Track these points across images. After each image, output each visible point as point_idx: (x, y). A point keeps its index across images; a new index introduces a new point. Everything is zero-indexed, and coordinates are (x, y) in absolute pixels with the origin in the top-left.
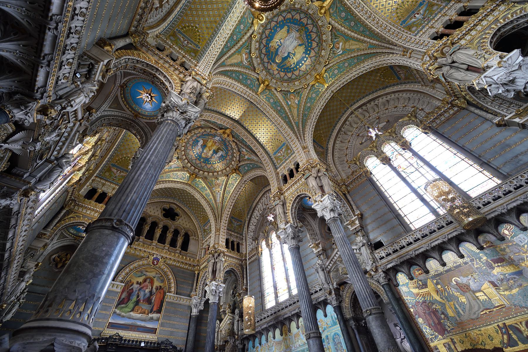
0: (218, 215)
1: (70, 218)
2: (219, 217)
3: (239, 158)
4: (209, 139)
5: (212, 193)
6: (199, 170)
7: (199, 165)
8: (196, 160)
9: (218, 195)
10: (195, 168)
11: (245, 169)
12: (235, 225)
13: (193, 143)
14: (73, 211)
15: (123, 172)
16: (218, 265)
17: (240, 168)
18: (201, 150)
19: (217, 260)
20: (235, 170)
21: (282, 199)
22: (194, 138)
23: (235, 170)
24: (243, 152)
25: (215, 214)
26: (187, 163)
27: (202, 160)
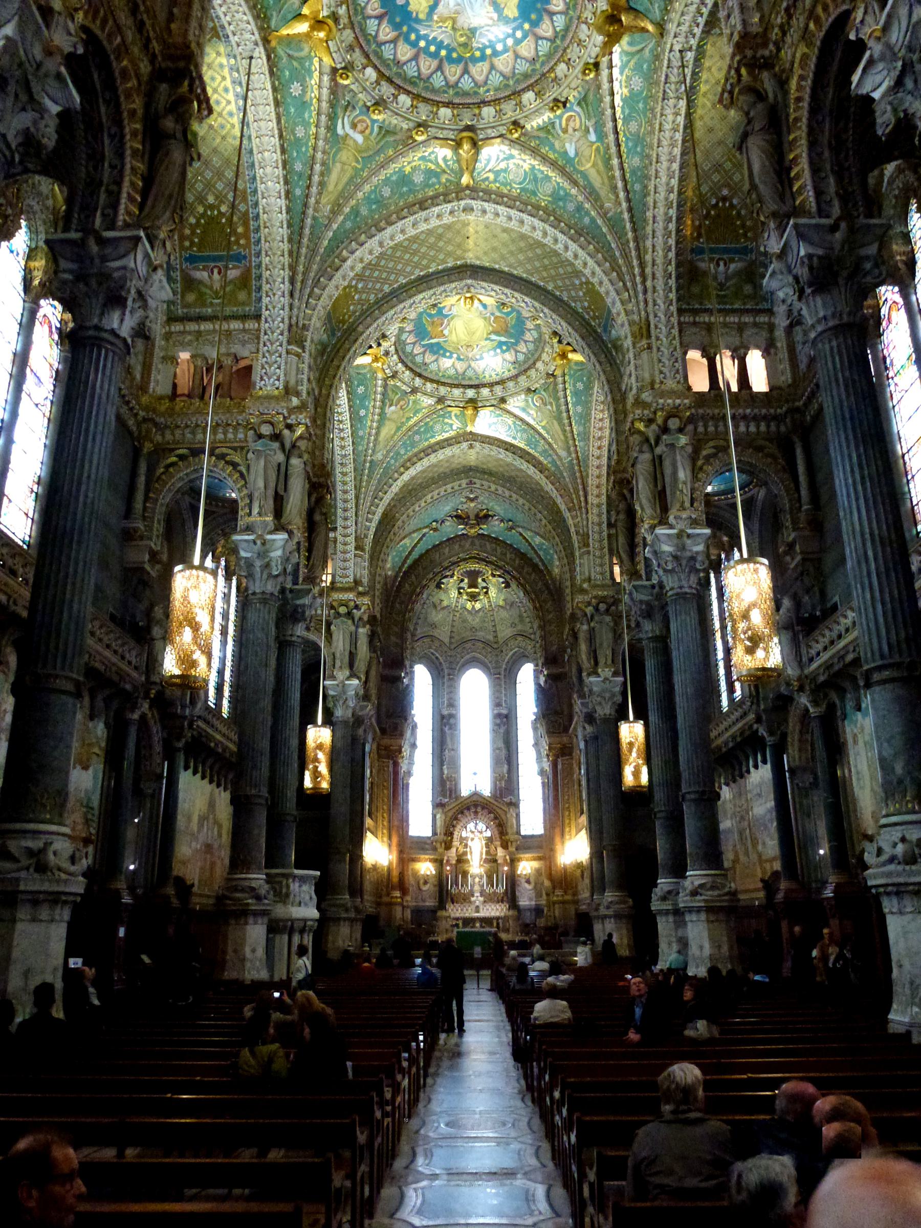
1: (167, 467)
8: (440, 68)
12: (721, 278)
14: (164, 450)
16: (667, 463)
19: (658, 450)
21: (771, 95)
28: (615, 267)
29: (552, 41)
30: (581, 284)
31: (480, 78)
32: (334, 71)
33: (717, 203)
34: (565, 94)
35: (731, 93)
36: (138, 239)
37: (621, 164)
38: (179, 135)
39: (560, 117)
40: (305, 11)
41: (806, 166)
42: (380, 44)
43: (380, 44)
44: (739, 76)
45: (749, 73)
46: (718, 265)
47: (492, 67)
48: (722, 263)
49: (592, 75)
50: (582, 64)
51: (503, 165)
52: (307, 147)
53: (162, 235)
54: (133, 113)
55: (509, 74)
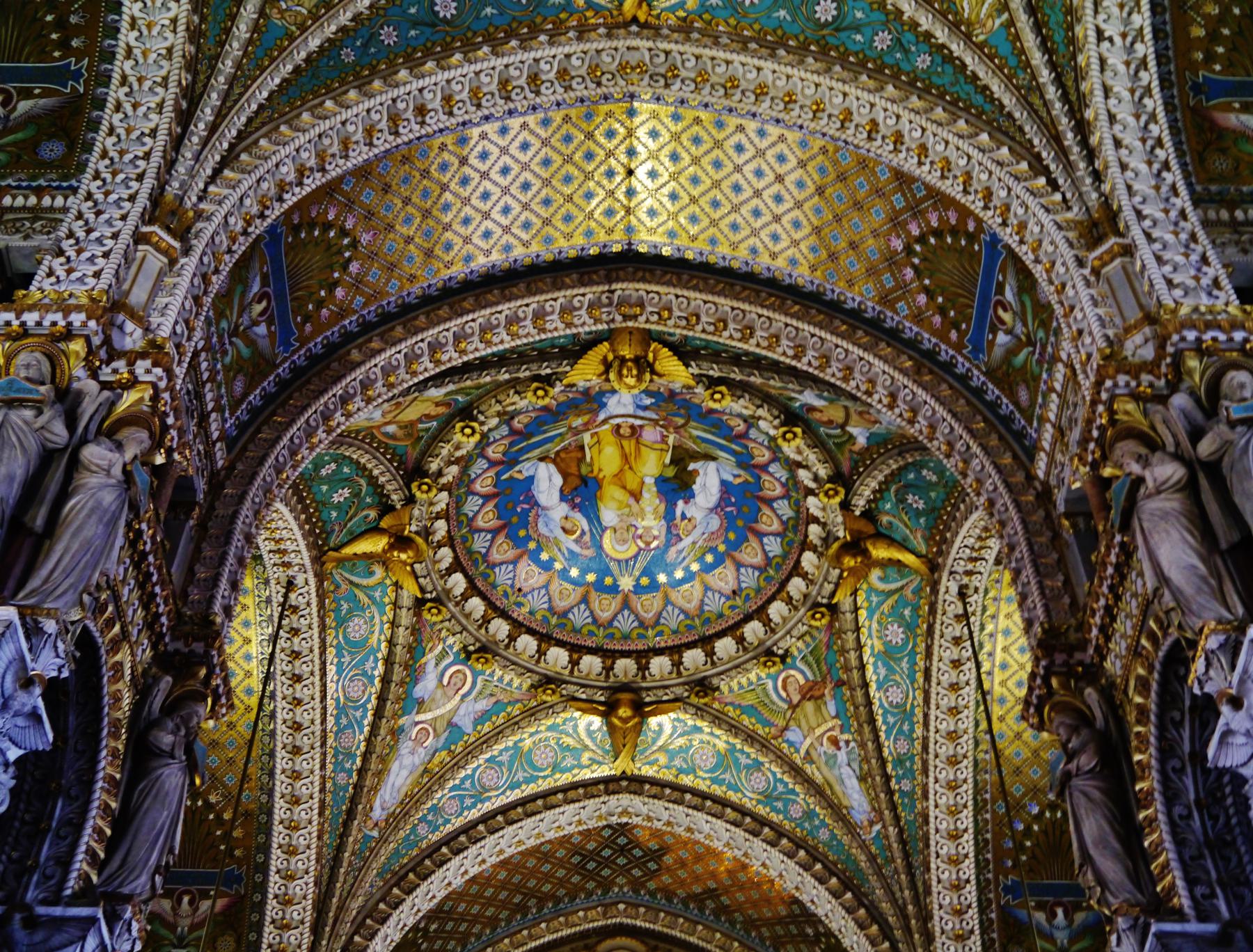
0: (905, 917)
2: (908, 930)
3: (829, 456)
4: (577, 432)
5: (796, 771)
6: (642, 657)
7: (625, 623)
8: (585, 600)
9: (846, 771)
10: (610, 655)
11: (919, 514)
12: (1062, 937)
13: (501, 512)
15: (205, 895)
17: (885, 519)
18: (581, 522)
20: (855, 546)
22: (484, 485)
23: (855, 546)
24: (817, 415)
25: (875, 915)
26: (541, 653)
27: (626, 583)
28: (875, 915)
29: (762, 570)
30: (817, 935)
31: (649, 616)
32: (419, 603)
33: (1042, 813)
34: (784, 644)
35: (1039, 711)
36: (93, 920)
37: (879, 748)
38: (180, 753)
39: (775, 679)
40: (383, 524)
41: (1166, 837)
42: (492, 566)
43: (492, 566)
44: (1049, 686)
45: (1065, 685)
46: (1055, 915)
47: (667, 601)
48: (1060, 912)
49: (824, 621)
50: (809, 604)
51: (681, 741)
52: (366, 710)
53: (128, 915)
54: (116, 724)
55: (693, 612)
